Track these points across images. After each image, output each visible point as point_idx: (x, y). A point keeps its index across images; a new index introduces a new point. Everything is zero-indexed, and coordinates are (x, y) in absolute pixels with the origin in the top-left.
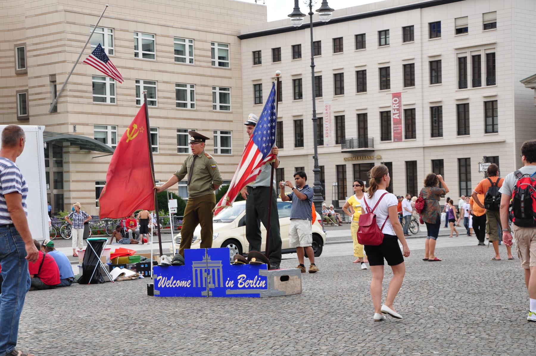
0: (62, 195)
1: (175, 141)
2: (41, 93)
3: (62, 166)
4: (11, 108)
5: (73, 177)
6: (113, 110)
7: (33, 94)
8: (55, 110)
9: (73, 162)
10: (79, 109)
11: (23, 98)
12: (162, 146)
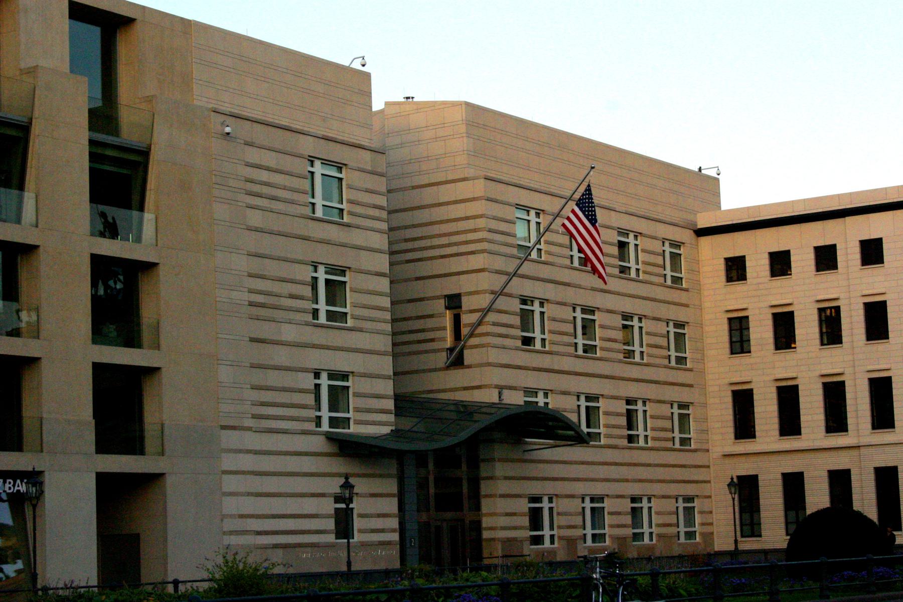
2: (423, 331)
8: (458, 362)
9: (500, 460)
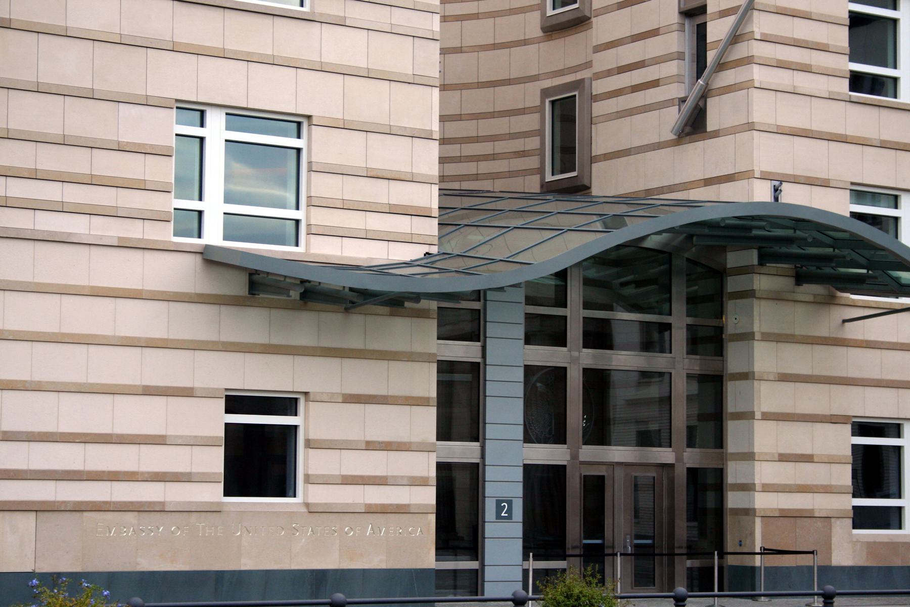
0: (720, 473)
3: (720, 351)
4: (523, 154)
5: (768, 397)
7: (609, 73)
8: (695, 125)
9: (767, 337)
10: (794, 114)
11: (566, 114)
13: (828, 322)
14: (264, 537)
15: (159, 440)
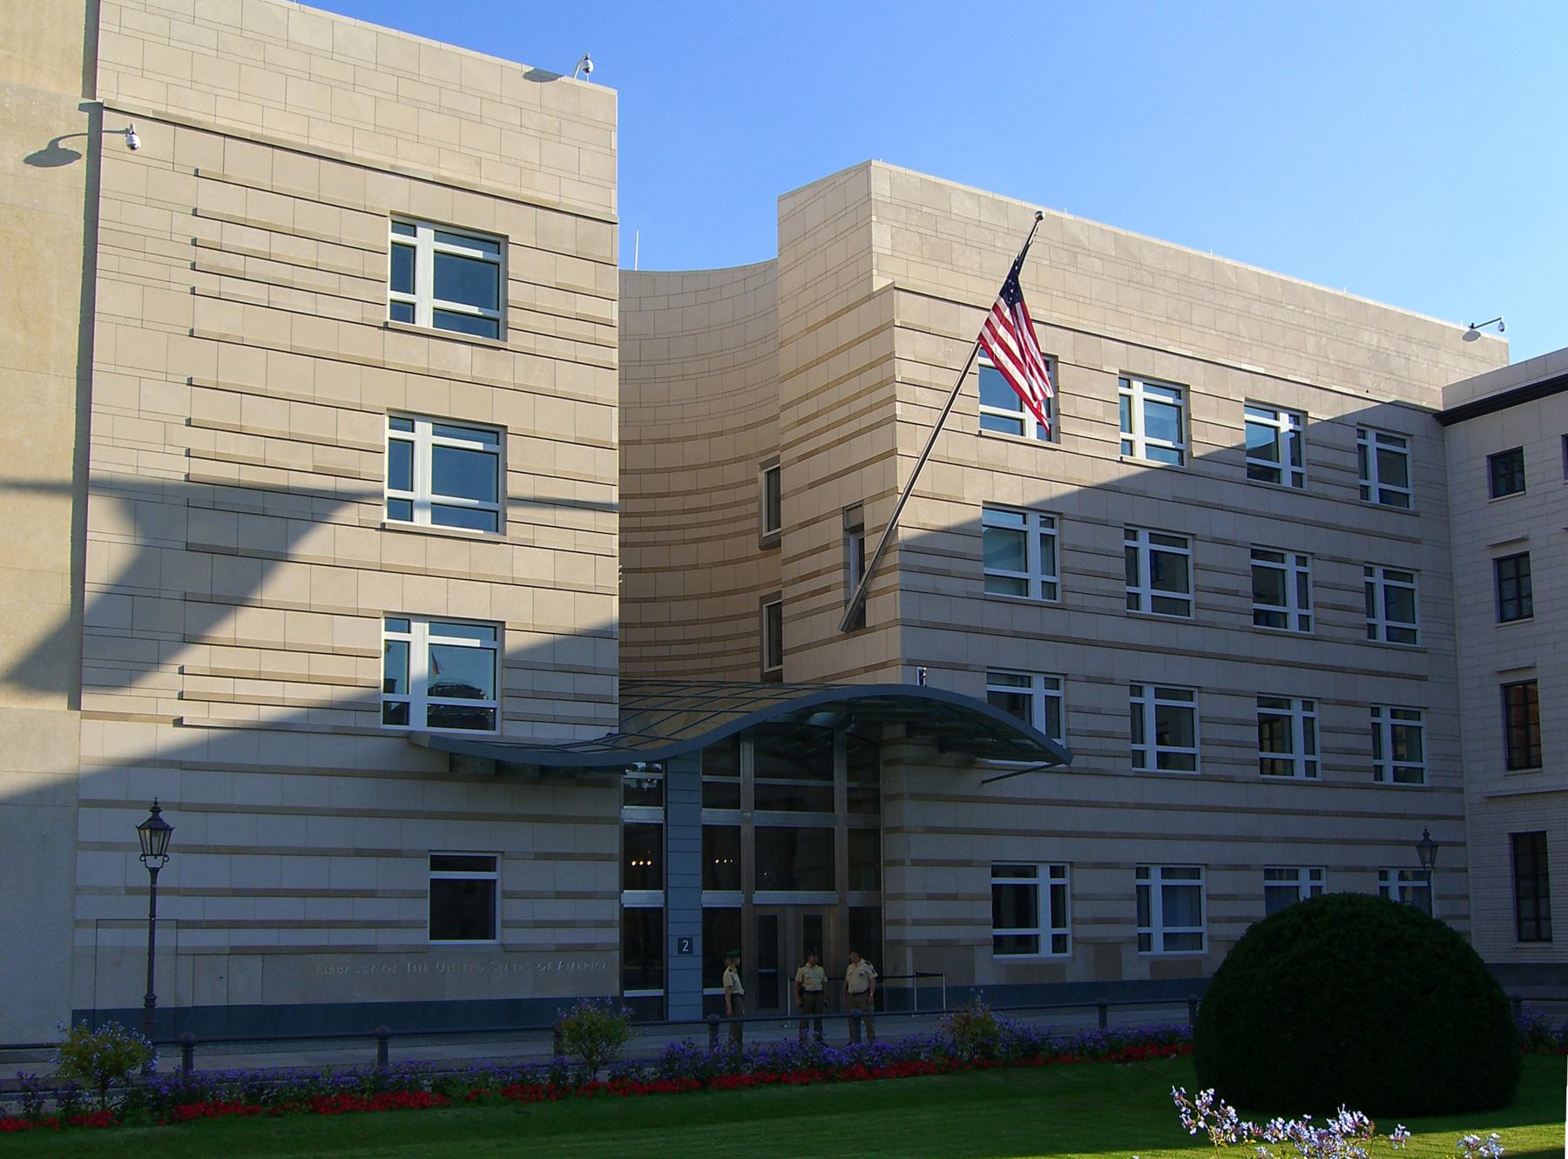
0: (878, 910)
1: (1252, 735)
3: (877, 810)
4: (746, 651)
6: (1053, 622)
7: (794, 582)
8: (856, 622)
9: (914, 796)
12: (1211, 751)
13: (970, 781)
14: (464, 972)
15: (371, 894)
